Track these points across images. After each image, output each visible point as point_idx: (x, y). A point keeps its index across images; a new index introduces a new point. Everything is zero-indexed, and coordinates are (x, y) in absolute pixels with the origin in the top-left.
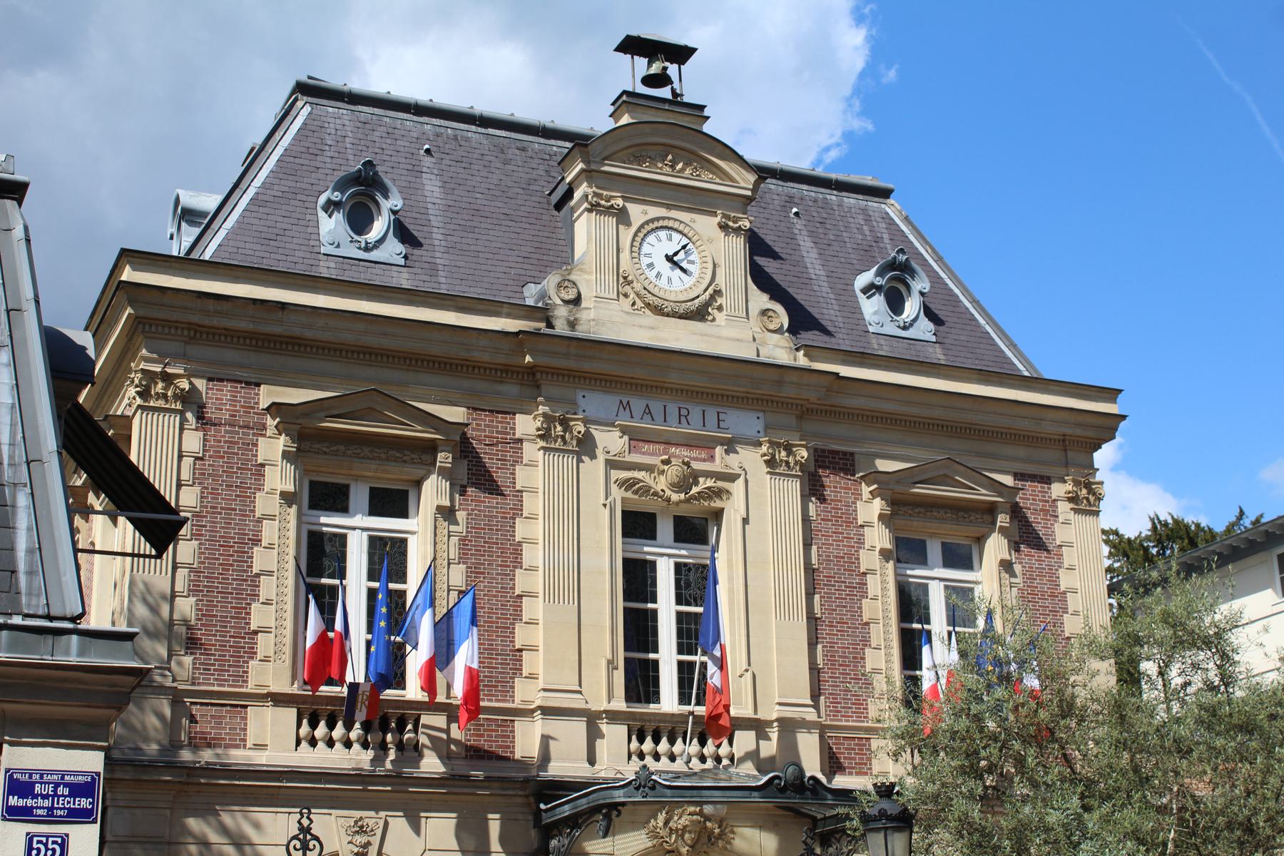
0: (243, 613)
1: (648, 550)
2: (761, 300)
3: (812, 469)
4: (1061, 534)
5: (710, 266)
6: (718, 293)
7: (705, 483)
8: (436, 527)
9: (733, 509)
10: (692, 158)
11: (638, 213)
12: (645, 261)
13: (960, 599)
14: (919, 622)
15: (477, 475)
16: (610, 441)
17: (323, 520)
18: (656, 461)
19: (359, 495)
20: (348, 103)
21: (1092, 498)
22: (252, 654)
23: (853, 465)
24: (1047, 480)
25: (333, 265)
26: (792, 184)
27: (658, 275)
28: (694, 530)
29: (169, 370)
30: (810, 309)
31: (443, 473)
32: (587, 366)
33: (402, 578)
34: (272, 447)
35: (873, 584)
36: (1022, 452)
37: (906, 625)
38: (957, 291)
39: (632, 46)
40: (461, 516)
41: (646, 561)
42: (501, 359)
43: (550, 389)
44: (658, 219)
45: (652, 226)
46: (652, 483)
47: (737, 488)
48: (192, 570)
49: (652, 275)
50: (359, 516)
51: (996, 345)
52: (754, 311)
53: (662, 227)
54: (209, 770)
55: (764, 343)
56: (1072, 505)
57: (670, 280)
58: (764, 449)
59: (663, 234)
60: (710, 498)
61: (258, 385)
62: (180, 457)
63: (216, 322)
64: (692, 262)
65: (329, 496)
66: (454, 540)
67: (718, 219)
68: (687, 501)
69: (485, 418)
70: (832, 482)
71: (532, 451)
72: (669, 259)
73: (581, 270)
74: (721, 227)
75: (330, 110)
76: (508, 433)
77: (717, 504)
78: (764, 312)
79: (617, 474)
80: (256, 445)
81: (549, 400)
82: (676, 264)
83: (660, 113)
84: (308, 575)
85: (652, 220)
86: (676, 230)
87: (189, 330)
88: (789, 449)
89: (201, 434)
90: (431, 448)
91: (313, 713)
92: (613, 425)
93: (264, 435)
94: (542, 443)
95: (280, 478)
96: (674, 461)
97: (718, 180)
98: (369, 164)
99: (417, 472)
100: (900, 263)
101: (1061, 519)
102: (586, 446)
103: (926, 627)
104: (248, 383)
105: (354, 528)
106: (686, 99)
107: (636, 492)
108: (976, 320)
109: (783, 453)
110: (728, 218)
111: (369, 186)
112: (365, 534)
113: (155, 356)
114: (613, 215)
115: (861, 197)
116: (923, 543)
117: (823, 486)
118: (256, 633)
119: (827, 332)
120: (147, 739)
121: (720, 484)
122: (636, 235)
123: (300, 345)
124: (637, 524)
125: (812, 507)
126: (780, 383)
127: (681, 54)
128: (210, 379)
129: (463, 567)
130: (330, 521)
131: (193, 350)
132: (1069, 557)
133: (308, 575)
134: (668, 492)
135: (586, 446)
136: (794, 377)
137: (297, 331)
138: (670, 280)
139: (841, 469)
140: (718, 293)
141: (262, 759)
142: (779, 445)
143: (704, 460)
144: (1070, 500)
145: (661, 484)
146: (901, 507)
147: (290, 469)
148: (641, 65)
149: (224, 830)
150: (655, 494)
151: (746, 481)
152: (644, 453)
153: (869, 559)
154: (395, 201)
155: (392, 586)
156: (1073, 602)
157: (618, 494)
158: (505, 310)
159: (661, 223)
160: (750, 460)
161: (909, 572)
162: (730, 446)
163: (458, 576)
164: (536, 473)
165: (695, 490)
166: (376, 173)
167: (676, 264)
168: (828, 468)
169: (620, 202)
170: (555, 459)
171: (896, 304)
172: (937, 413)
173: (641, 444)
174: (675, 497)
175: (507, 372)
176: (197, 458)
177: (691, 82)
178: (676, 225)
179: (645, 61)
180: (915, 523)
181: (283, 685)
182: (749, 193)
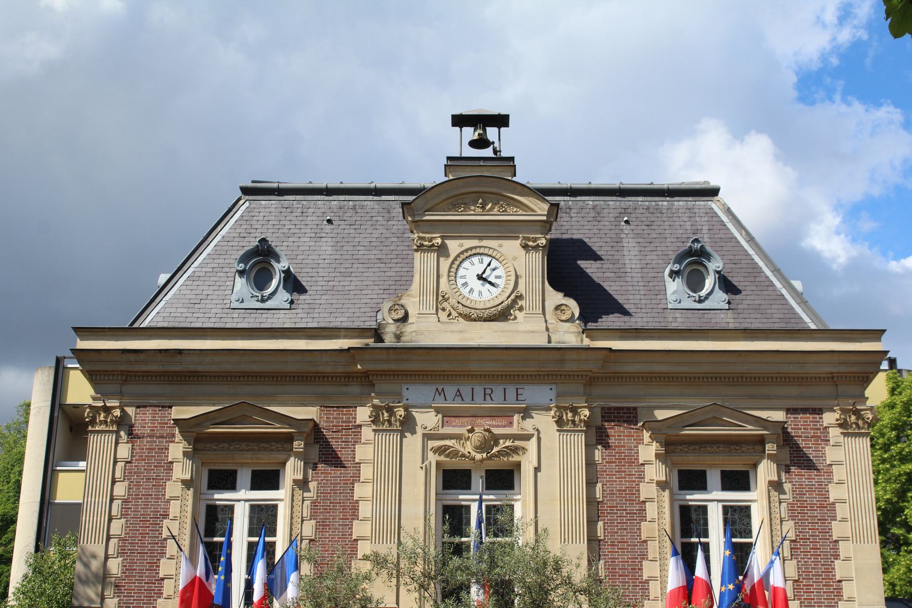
0: (154, 566)
1: (463, 497)
2: (555, 298)
3: (599, 423)
4: (831, 454)
5: (513, 278)
6: (520, 297)
7: (503, 444)
8: (293, 495)
9: (528, 463)
10: (499, 199)
11: (454, 246)
12: (460, 281)
14: (699, 536)
16: (427, 419)
17: (216, 496)
18: (463, 431)
19: (244, 477)
20: (278, 195)
21: (860, 423)
22: (160, 594)
23: (636, 417)
24: (819, 411)
25: (236, 315)
26: (630, 198)
27: (471, 291)
28: (503, 479)
29: (108, 405)
30: (616, 297)
31: (298, 455)
33: (273, 533)
34: (177, 449)
35: (651, 510)
36: (793, 390)
37: (686, 540)
38: (761, 264)
39: (459, 121)
40: (313, 485)
41: (462, 506)
42: (340, 369)
43: (381, 386)
44: (471, 249)
45: (466, 254)
46: (462, 449)
47: (532, 445)
48: (120, 539)
49: (465, 291)
50: (243, 491)
51: (787, 303)
53: (475, 254)
56: (841, 430)
57: (480, 293)
58: (552, 413)
59: (475, 259)
60: (508, 454)
61: (171, 407)
62: (115, 462)
64: (497, 277)
65: (224, 480)
66: (307, 503)
67: (519, 241)
69: (334, 413)
70: (616, 432)
71: (367, 433)
72: (480, 277)
73: (409, 295)
74: (523, 247)
75: (263, 202)
76: (351, 422)
77: (515, 458)
78: (558, 308)
79: (433, 444)
80: (168, 449)
81: (379, 395)
82: (485, 280)
83: (476, 169)
84: (206, 536)
85: (466, 251)
86: (486, 255)
87: (122, 375)
88: (574, 410)
89: (130, 445)
90: (289, 438)
92: (431, 407)
93: (173, 442)
94: (374, 427)
95: (182, 470)
96: (477, 429)
97: (521, 212)
98: (263, 241)
99: (281, 457)
100: (696, 251)
101: (831, 443)
102: (408, 425)
103: (702, 540)
104: (163, 407)
105: (239, 501)
106: (504, 154)
107: (447, 456)
108: (773, 285)
109: (570, 415)
110: (529, 239)
111: (266, 255)
112: (247, 504)
113: (99, 395)
114: (434, 251)
115: (690, 199)
117: (608, 436)
118: (163, 579)
119: (626, 313)
121: (517, 443)
122: (453, 263)
123: (198, 376)
124: (454, 478)
125: (598, 454)
126: (562, 361)
127: (501, 121)
128: (138, 407)
129: (313, 522)
131: (127, 388)
132: (838, 473)
133: (206, 536)
134: (473, 454)
136: (574, 356)
137: (192, 368)
138: (480, 293)
139: (625, 421)
140: (520, 297)
142: (565, 408)
143: (504, 426)
144: (841, 426)
145: (468, 448)
146: (671, 445)
147: (189, 463)
148: (470, 133)
150: (463, 456)
151: (539, 439)
152: (454, 426)
153: (647, 490)
155: (268, 539)
156: (841, 511)
157: (433, 458)
158: (342, 334)
159: (474, 251)
160: (544, 422)
161: (688, 497)
162: (526, 413)
163: (309, 529)
164: (368, 449)
165: (495, 450)
166: (269, 246)
167: (485, 280)
168: (614, 421)
169: (439, 241)
171: (695, 282)
172: (706, 368)
173: (452, 419)
174: (478, 456)
175: (349, 377)
176: (127, 462)
177: (506, 141)
178: (486, 251)
179: (472, 129)
180: (691, 458)
182: (545, 218)
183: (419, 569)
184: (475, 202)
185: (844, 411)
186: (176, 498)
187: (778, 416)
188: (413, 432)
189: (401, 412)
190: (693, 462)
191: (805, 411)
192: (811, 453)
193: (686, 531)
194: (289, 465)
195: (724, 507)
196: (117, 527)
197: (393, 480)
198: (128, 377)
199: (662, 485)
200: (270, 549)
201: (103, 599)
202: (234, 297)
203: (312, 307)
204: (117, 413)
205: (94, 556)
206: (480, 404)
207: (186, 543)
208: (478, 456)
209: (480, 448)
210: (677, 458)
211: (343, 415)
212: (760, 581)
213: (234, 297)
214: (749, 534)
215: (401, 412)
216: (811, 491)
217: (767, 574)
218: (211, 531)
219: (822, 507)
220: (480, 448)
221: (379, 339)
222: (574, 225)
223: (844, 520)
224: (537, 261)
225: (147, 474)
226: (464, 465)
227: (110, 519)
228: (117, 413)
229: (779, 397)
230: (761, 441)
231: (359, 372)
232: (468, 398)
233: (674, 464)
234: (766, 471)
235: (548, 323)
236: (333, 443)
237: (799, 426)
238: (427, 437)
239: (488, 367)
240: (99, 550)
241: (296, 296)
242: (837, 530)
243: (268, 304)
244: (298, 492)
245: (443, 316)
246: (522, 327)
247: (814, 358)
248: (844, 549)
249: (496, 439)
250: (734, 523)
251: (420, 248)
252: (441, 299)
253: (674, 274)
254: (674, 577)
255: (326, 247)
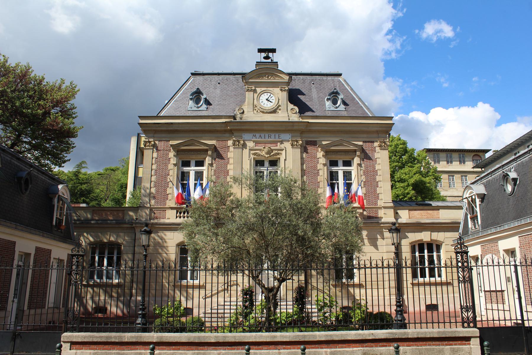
0: (165, 190)
1: (262, 169)
2: (291, 106)
4: (376, 155)
6: (280, 106)
7: (274, 152)
9: (282, 158)
10: (273, 75)
11: (259, 90)
12: (261, 101)
13: (199, 176)
15: (218, 155)
16: (250, 144)
18: (262, 148)
19: (193, 163)
24: (373, 142)
27: (264, 104)
28: (274, 163)
31: (209, 156)
32: (243, 128)
33: (202, 180)
34: (172, 154)
35: (321, 173)
36: (365, 136)
38: (355, 97)
39: (260, 51)
40: (214, 165)
42: (223, 129)
43: (235, 134)
49: (262, 104)
52: (289, 109)
54: (157, 224)
55: (291, 117)
59: (265, 94)
62: (152, 158)
63: (158, 129)
65: (187, 164)
68: (270, 157)
70: (310, 148)
71: (231, 149)
72: (267, 100)
77: (278, 156)
78: (292, 109)
79: (252, 152)
81: (235, 137)
88: (297, 141)
90: (207, 151)
91: (179, 211)
95: (173, 161)
98: (198, 89)
99: (204, 156)
102: (244, 146)
116: (337, 161)
119: (313, 111)
120: (143, 218)
121: (279, 152)
124: (259, 163)
125: (304, 155)
126: (293, 126)
127: (273, 51)
130: (334, 169)
131: (155, 135)
132: (379, 161)
135: (244, 146)
136: (297, 124)
137: (176, 128)
140: (280, 106)
141: (167, 221)
144: (379, 146)
145: (263, 153)
146: (327, 153)
147: (175, 158)
148: (264, 55)
149: (158, 236)
153: (320, 166)
154: (205, 96)
156: (379, 173)
162: (282, 142)
164: (232, 154)
170: (237, 150)
171: (335, 102)
174: (267, 156)
177: (275, 57)
181: (173, 205)
183: (248, 182)
184: (265, 76)
185: (381, 142)
186: (172, 169)
187: (361, 143)
188: (246, 148)
189: (242, 142)
190: (334, 158)
191: (369, 142)
192: (370, 155)
193: (332, 179)
194: (207, 159)
195: (344, 172)
196: (153, 178)
197: (240, 160)
198: (156, 132)
199: (324, 165)
200: (201, 185)
201: (150, 200)
202: (189, 107)
203: (213, 110)
204: (153, 143)
205: (148, 188)
206: (267, 139)
207: (175, 183)
208: (267, 156)
209: (267, 153)
210: (329, 156)
211: (224, 143)
212: (354, 194)
213: (189, 107)
214: (351, 180)
215: (242, 142)
216: (370, 167)
217: (357, 192)
218: (183, 179)
219: (373, 171)
220: (267, 153)
221: (235, 119)
222: (296, 84)
223: (380, 175)
224: (285, 95)
225: (163, 162)
226: (262, 159)
227: (151, 176)
228: (153, 143)
229: (360, 138)
230: (355, 151)
231: (229, 130)
232: (263, 137)
233: (328, 158)
234: (356, 160)
235: (289, 114)
236: (221, 152)
237: (367, 146)
238: (250, 150)
239: (269, 128)
240: (148, 185)
241: (208, 106)
242: (378, 178)
243: (200, 109)
244: (210, 167)
245: (255, 112)
246: (280, 115)
247: (371, 125)
248: (380, 184)
249: (272, 150)
250: (346, 176)
251: (248, 90)
252: (254, 106)
253: (328, 99)
254: (328, 193)
255: (218, 91)
